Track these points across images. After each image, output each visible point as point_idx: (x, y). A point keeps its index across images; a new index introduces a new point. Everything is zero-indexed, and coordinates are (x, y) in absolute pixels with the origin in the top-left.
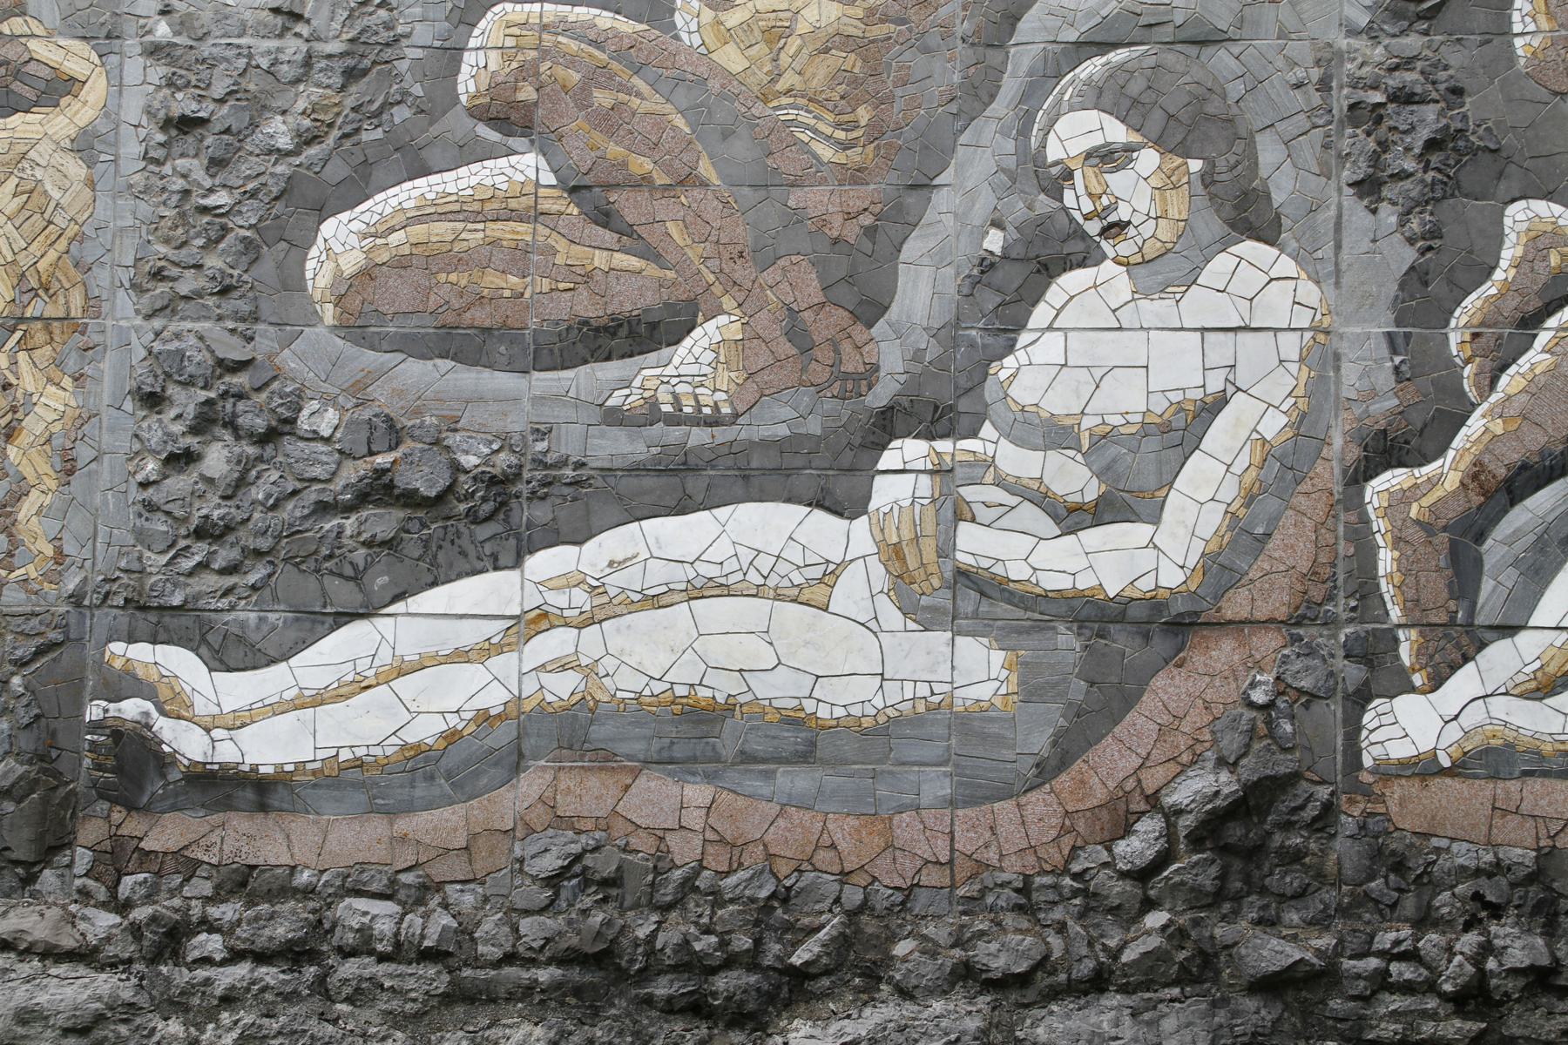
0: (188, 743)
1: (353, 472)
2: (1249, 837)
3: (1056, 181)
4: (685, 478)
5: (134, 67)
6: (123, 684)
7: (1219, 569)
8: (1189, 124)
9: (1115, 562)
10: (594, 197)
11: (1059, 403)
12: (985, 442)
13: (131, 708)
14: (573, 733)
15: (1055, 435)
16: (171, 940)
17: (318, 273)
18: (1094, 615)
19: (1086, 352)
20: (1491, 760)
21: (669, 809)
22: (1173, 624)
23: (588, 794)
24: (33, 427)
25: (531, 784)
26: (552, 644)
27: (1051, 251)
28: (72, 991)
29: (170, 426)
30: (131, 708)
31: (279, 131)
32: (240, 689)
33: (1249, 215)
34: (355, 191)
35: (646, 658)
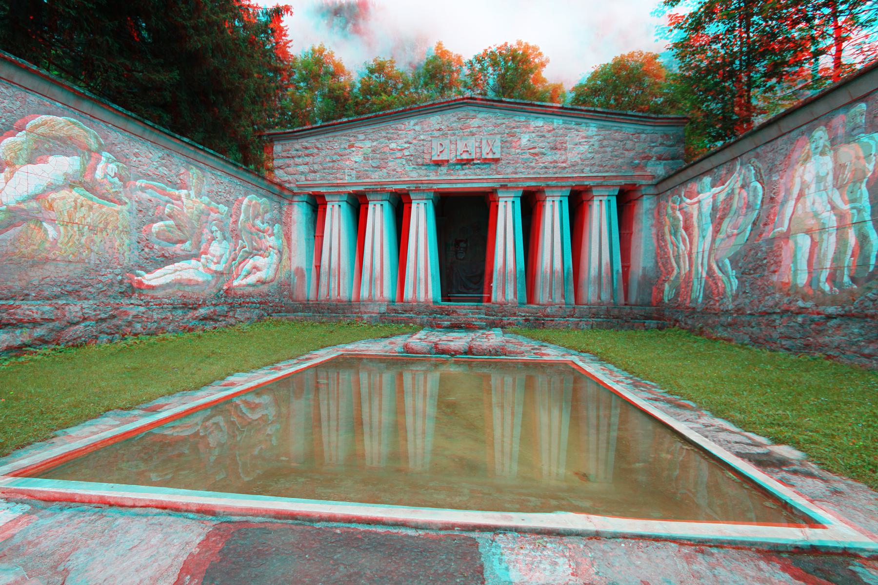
0: (146, 282)
1: (160, 253)
2: (227, 291)
3: (212, 232)
4: (187, 257)
5: (134, 203)
6: (138, 275)
7: (225, 269)
8: (222, 230)
9: (220, 268)
10: (179, 227)
11: (214, 253)
12: (209, 256)
13: (140, 278)
14: (179, 283)
15: (214, 256)
16: (147, 303)
17: (153, 230)
18: (216, 272)
19: (216, 248)
20: (240, 285)
21: (188, 289)
22: (222, 273)
23: (182, 288)
24: (126, 244)
25: (177, 287)
26: (178, 273)
27: (213, 239)
28: (142, 309)
29: (140, 246)
30: (140, 278)
31: (150, 213)
32: (147, 276)
33: (225, 238)
34: (157, 222)
35: (186, 275)
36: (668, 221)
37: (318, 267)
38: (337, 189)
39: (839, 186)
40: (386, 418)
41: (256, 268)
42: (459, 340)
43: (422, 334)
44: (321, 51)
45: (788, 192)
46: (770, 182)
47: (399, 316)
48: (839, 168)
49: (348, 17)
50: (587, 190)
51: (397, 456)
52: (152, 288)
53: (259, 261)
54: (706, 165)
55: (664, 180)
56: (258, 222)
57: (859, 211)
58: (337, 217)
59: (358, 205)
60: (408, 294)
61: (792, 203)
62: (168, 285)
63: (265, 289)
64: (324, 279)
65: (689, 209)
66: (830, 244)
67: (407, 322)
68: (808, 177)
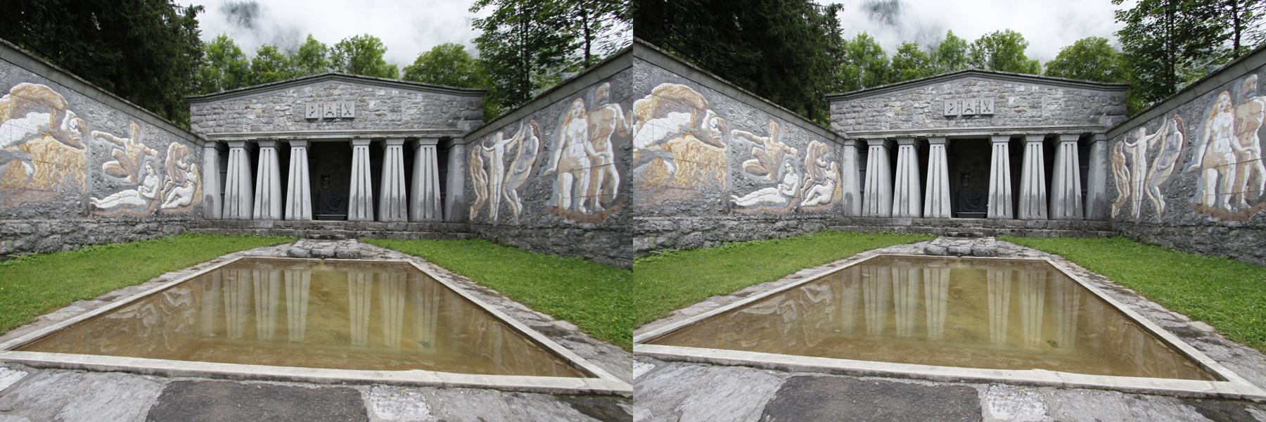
36: (473, 162)
37: (223, 195)
38: (238, 138)
39: (592, 140)
40: (274, 303)
41: (178, 196)
42: (328, 247)
43: (300, 243)
44: (224, 39)
45: (557, 143)
46: (544, 137)
47: (283, 230)
48: (591, 128)
49: (246, 14)
50: (416, 140)
51: (282, 332)
52: (103, 210)
53: (179, 190)
54: (499, 124)
55: (470, 134)
56: (180, 162)
57: (606, 157)
58: (238, 158)
59: (253, 151)
60: (288, 214)
61: (559, 151)
62: (114, 208)
63: (184, 210)
64: (227, 203)
65: (486, 154)
66: (585, 180)
67: (288, 234)
68: (571, 133)
